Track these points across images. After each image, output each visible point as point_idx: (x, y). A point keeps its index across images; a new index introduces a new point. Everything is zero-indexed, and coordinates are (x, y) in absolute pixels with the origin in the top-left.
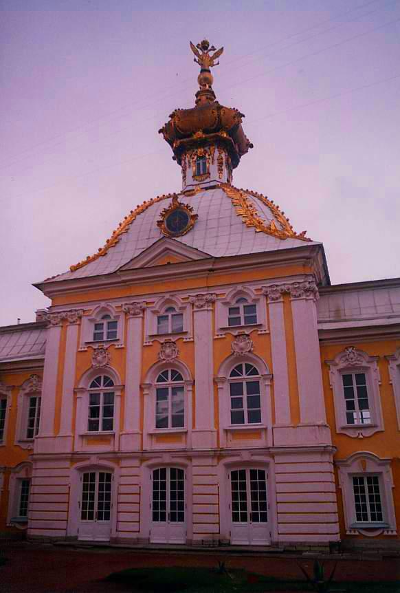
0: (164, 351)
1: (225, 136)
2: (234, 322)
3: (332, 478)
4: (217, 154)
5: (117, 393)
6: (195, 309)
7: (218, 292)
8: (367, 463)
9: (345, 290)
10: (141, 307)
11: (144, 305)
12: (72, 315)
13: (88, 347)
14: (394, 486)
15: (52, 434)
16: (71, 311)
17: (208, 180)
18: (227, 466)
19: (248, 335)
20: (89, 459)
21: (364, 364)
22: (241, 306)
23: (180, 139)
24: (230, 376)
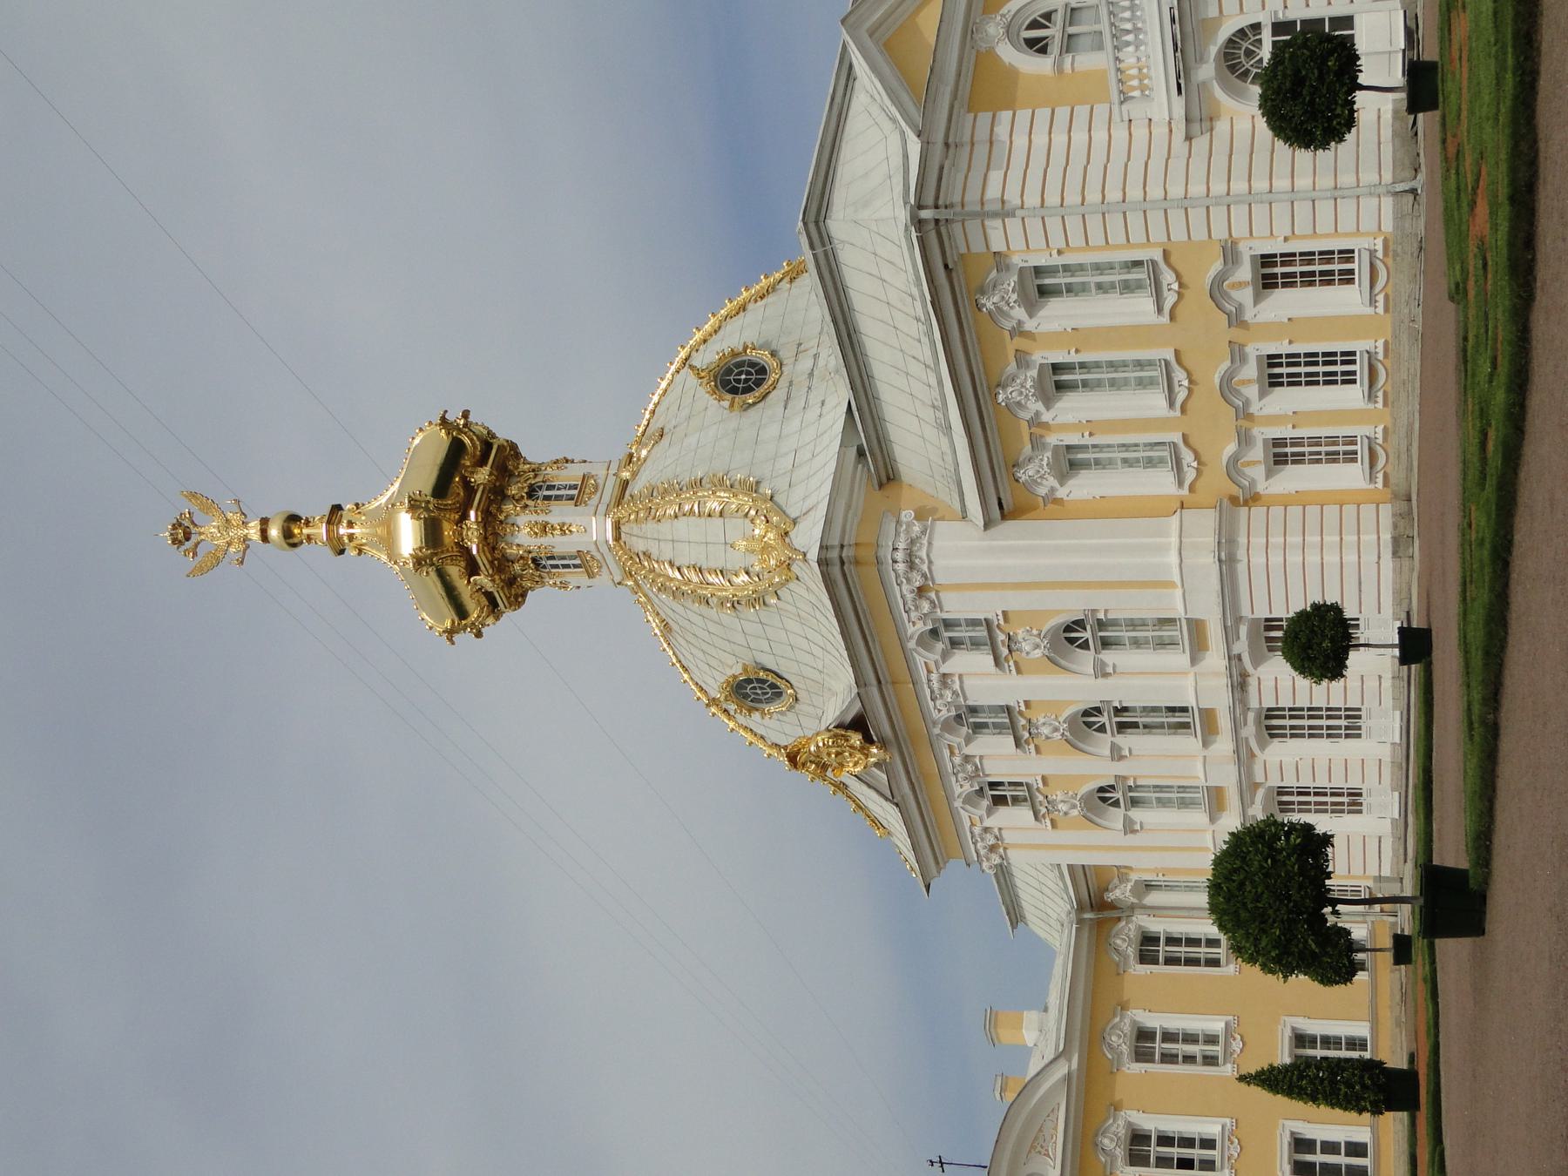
11: (957, 760)
16: (975, 844)
17: (598, 557)
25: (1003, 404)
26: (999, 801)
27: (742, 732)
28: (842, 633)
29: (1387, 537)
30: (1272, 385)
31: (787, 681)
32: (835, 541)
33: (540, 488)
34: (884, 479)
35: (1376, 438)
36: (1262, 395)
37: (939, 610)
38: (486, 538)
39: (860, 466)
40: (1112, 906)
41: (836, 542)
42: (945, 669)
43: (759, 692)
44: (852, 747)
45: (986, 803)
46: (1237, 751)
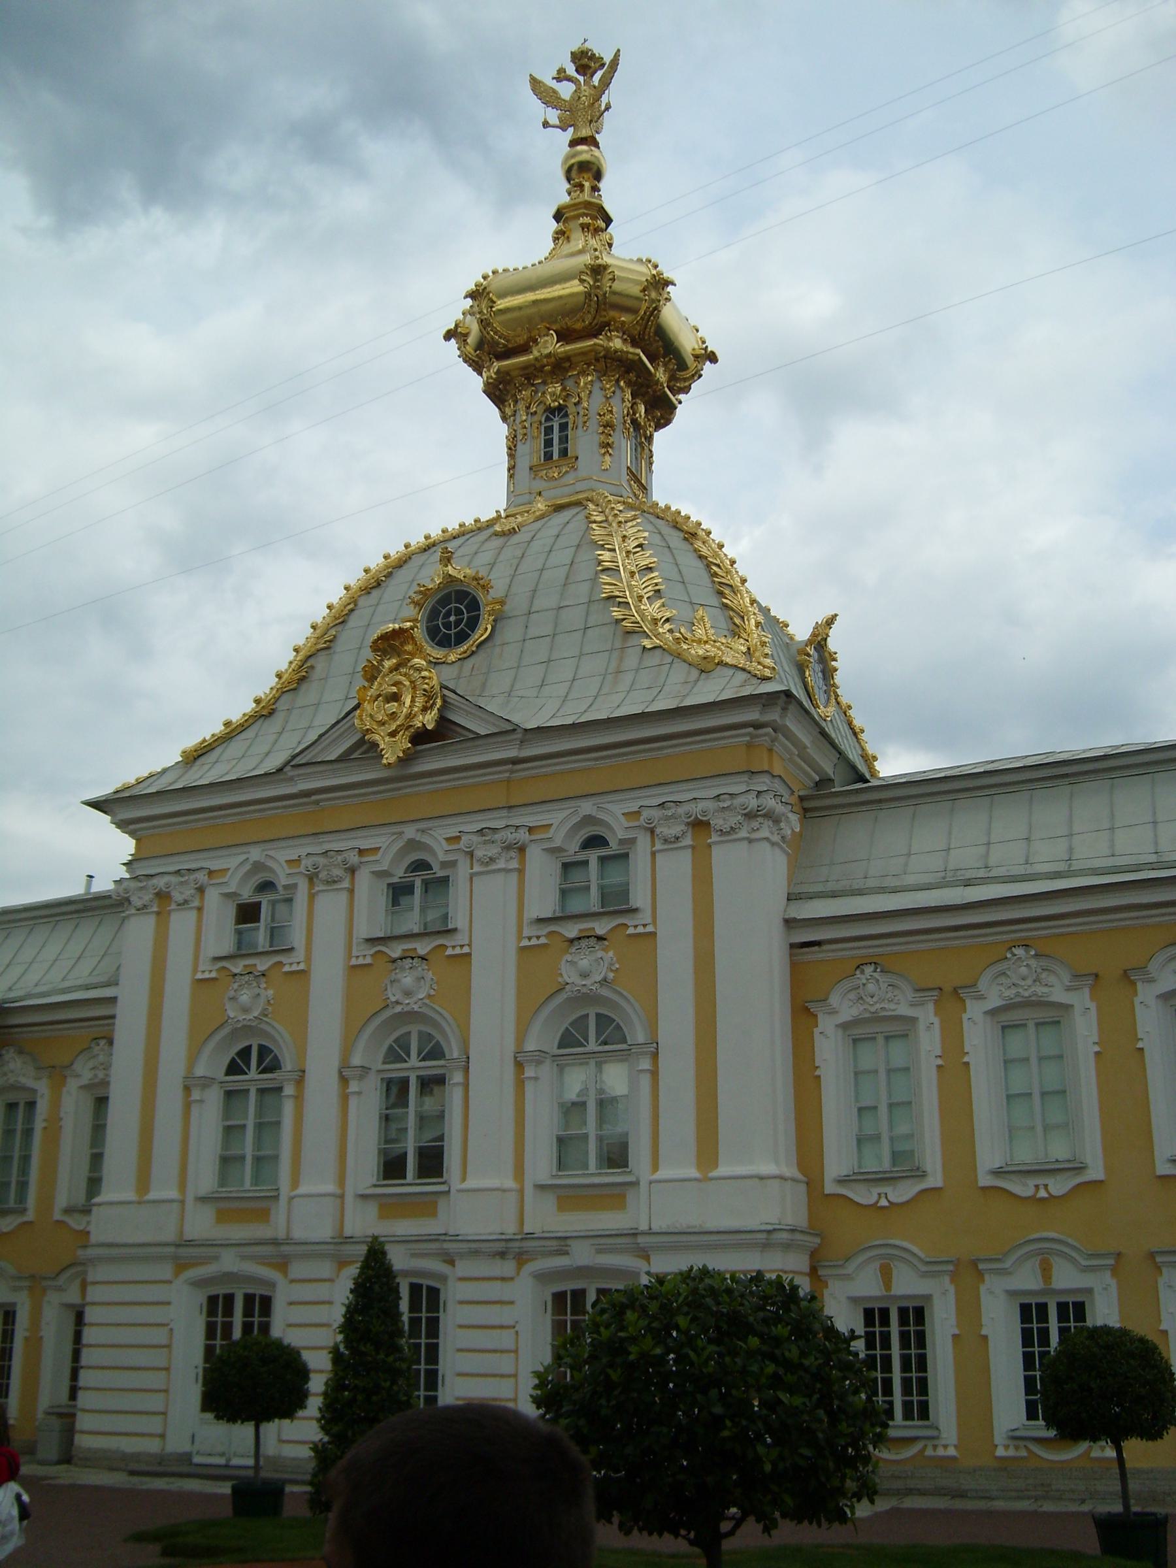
1: (617, 344)
5: (289, 1090)
6: (477, 868)
7: (531, 821)
8: (895, 1272)
9: (880, 801)
10: (345, 862)
11: (354, 859)
13: (218, 970)
14: (957, 1332)
15: (131, 1196)
16: (178, 872)
19: (600, 938)
20: (216, 1258)
21: (904, 1010)
23: (500, 357)
24: (559, 1047)
25: (1009, 955)
26: (248, 914)
30: (1025, 1310)
34: (807, 805)
35: (935, 1447)
36: (1012, 1294)
43: (452, 618)
45: (247, 895)
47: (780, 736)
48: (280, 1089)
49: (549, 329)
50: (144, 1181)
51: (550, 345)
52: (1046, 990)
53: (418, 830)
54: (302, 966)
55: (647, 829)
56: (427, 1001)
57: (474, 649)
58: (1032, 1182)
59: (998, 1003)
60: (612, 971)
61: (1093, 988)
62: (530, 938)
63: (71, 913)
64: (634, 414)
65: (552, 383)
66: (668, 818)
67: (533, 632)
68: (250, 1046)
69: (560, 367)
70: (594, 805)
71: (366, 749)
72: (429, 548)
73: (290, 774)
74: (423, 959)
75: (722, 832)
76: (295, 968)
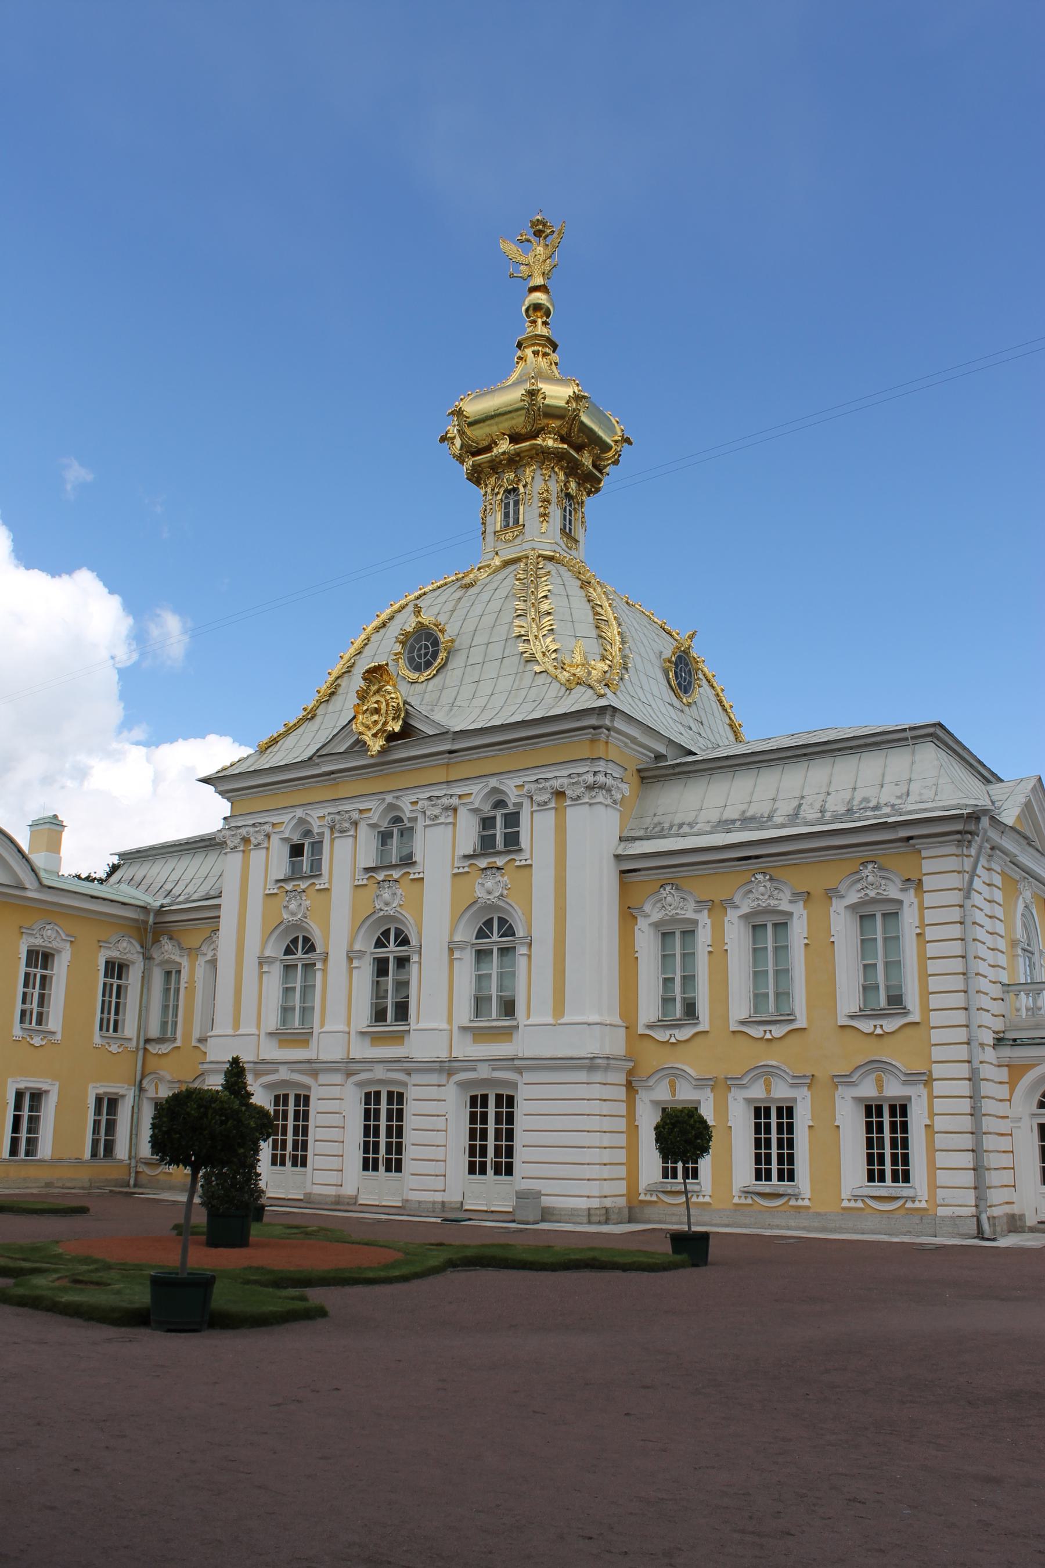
0: (382, 895)
1: (550, 443)
2: (487, 844)
3: (622, 1108)
4: (539, 485)
5: (319, 966)
9: (689, 772)
11: (355, 816)
12: (257, 832)
15: (230, 1032)
16: (254, 825)
18: (463, 1085)
19: (498, 868)
20: (277, 1071)
21: (690, 914)
22: (499, 815)
23: (474, 454)
25: (753, 879)
26: (296, 851)
27: (363, 637)
28: (522, 722)
29: (608, 1203)
30: (757, 1110)
31: (435, 675)
32: (619, 724)
33: (570, 505)
34: (643, 774)
35: (698, 1196)
36: (749, 1101)
37: (535, 808)
38: (543, 453)
39: (653, 756)
40: (156, 941)
41: (616, 725)
42: (462, 812)
44: (385, 723)
45: (296, 839)
46: (353, 1061)
47: (612, 733)
48: (314, 964)
49: (504, 434)
50: (237, 1024)
51: (504, 446)
52: (776, 902)
53: (394, 797)
54: (326, 886)
55: (528, 796)
56: (398, 909)
57: (435, 672)
58: (762, 1028)
59: (748, 910)
60: (506, 889)
61: (805, 902)
62: (459, 868)
63: (203, 847)
64: (567, 489)
65: (508, 472)
66: (540, 789)
67: (471, 661)
68: (298, 937)
69: (514, 462)
70: (498, 780)
71: (360, 745)
72: (421, 596)
73: (316, 761)
74: (396, 881)
75: (572, 799)
76: (322, 887)
